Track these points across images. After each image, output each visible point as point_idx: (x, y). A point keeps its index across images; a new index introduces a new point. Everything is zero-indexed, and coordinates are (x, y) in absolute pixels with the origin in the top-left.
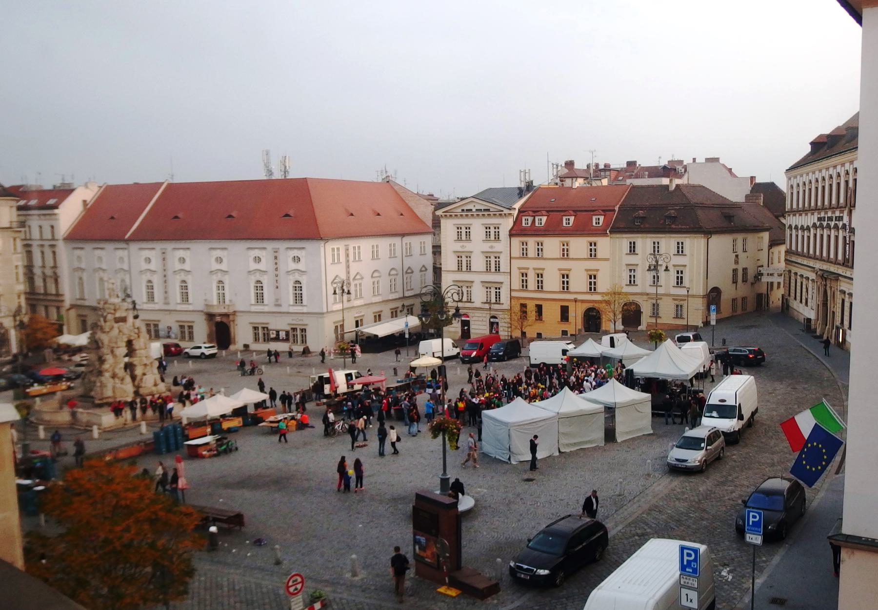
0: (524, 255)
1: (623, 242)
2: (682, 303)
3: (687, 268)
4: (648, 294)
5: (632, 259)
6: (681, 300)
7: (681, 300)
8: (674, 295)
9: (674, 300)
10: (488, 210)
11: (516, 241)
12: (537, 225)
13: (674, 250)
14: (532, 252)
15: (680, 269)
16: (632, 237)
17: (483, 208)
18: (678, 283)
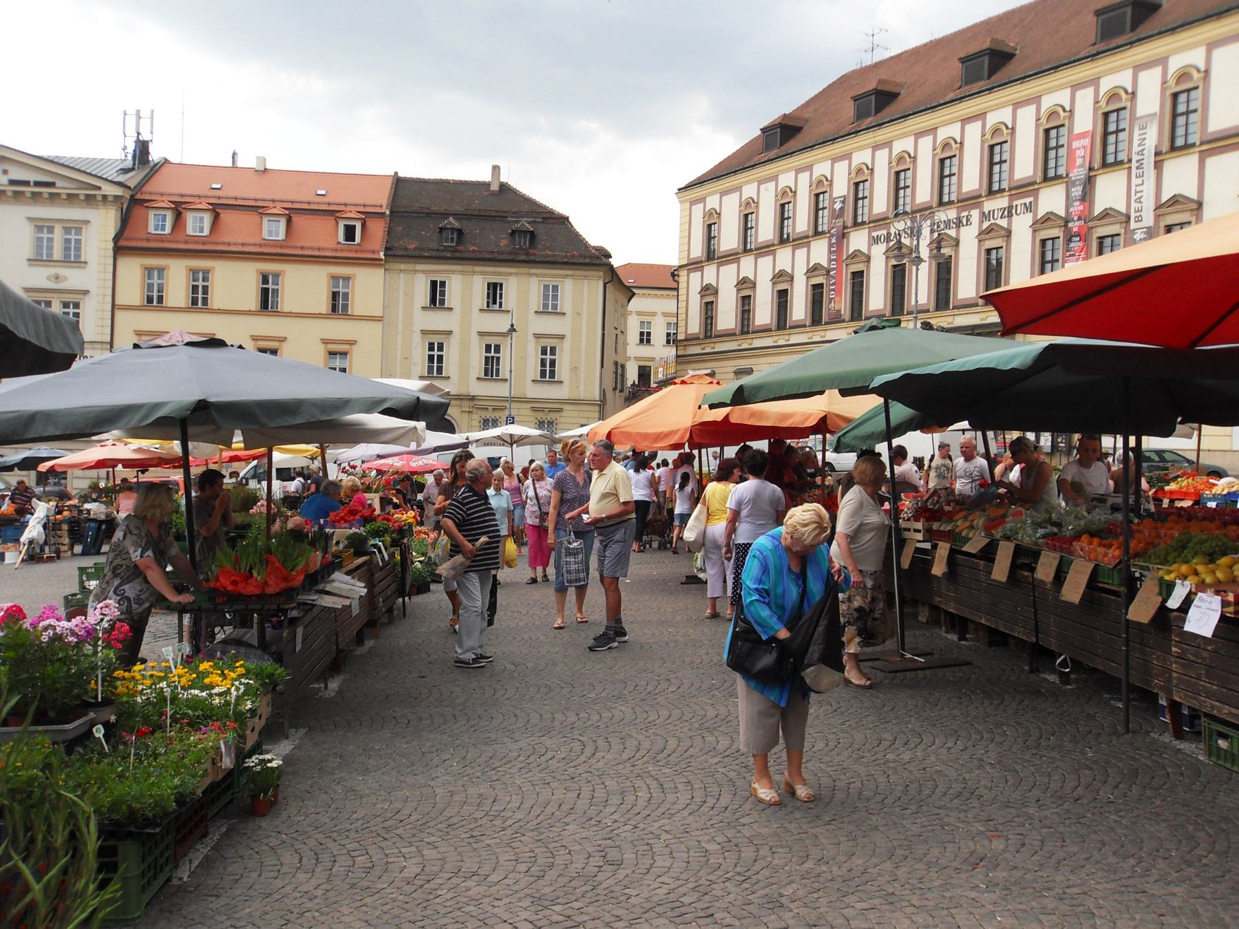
0: (154, 300)
1: (418, 283)
2: (552, 416)
3: (567, 343)
4: (473, 398)
5: (437, 321)
6: (551, 410)
7: (551, 410)
8: (534, 400)
9: (534, 409)
10: (52, 185)
11: (131, 269)
12: (190, 231)
13: (535, 301)
14: (177, 293)
15: (549, 343)
16: (439, 271)
17: (32, 177)
18: (543, 374)
